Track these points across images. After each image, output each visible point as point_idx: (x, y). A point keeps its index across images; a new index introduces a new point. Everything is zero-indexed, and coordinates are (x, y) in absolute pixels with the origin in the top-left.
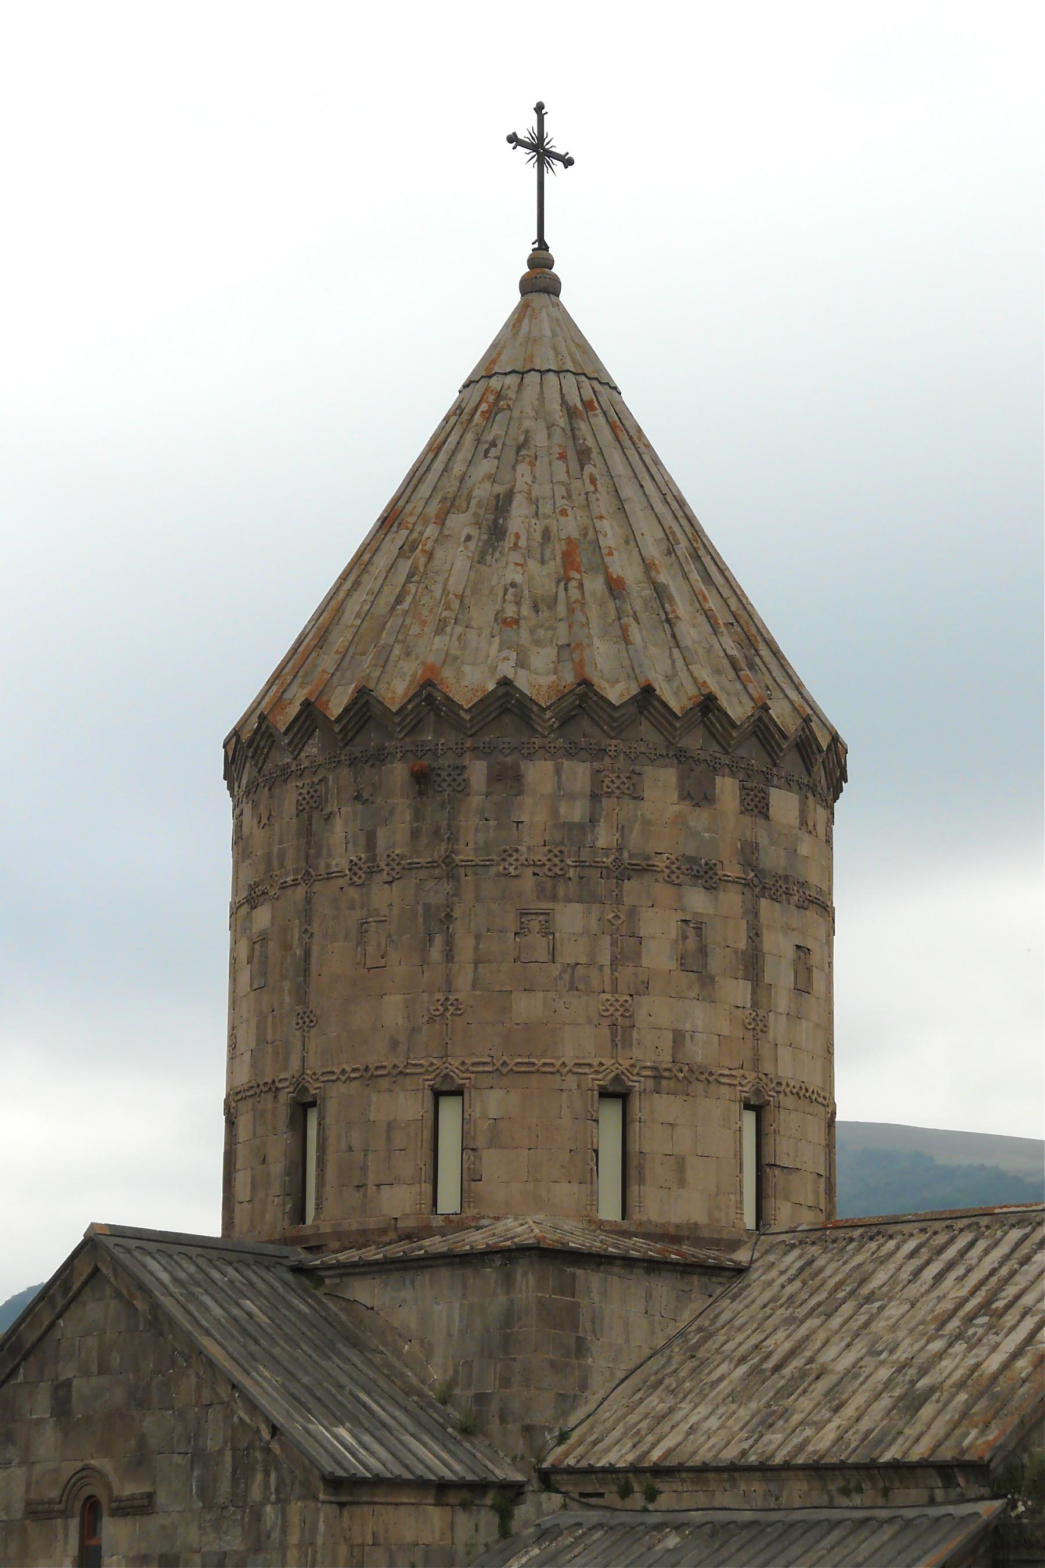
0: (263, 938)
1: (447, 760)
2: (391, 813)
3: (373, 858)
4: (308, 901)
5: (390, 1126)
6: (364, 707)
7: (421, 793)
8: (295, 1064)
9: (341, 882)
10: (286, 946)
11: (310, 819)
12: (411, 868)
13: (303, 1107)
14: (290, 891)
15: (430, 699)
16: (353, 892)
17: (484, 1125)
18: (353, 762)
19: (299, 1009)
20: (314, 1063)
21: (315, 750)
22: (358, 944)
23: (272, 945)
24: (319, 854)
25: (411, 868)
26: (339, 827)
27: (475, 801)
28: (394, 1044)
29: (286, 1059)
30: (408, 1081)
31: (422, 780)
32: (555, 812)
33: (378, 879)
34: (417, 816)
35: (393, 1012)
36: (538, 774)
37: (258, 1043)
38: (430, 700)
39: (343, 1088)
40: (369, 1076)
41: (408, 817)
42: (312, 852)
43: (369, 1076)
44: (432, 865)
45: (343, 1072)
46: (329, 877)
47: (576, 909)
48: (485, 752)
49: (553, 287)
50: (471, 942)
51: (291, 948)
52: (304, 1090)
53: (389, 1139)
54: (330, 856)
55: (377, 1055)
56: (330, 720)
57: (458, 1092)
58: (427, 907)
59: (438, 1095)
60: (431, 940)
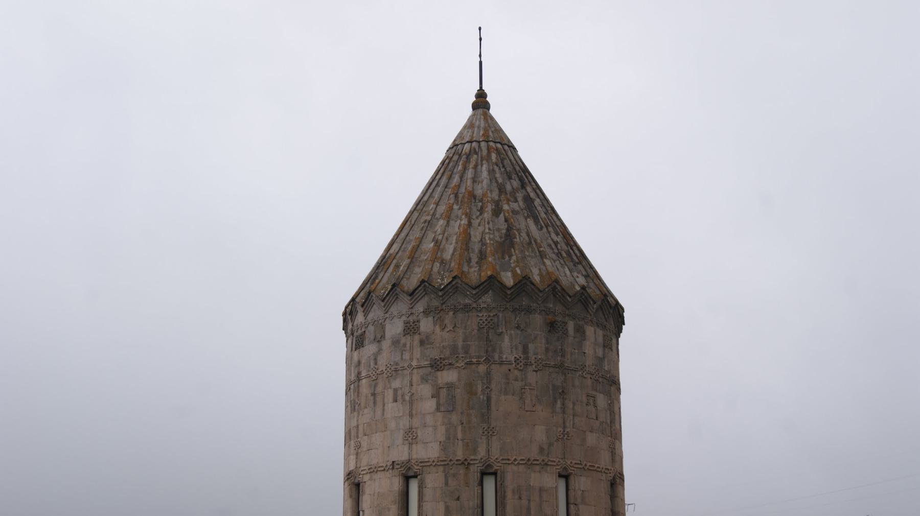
0: (450, 386)
1: (559, 319)
2: (535, 338)
3: (527, 358)
4: (488, 374)
5: (541, 490)
6: (524, 284)
7: (550, 331)
8: (482, 452)
9: (510, 367)
10: (472, 393)
11: (488, 333)
12: (546, 366)
13: (483, 474)
14: (474, 366)
15: (555, 289)
16: (516, 372)
17: (580, 493)
18: (514, 310)
19: (485, 425)
20: (495, 453)
21: (489, 300)
22: (521, 398)
23: (459, 392)
24: (494, 350)
25: (546, 366)
26: (507, 339)
27: (571, 339)
28: (541, 450)
29: (475, 451)
30: (549, 468)
31: (552, 326)
32: (595, 352)
33: (530, 368)
34: (547, 342)
35: (540, 434)
36: (590, 330)
37: (448, 438)
38: (554, 288)
39: (515, 468)
40: (529, 464)
41: (544, 341)
42: (490, 349)
43: (529, 464)
44: (555, 366)
45: (515, 460)
46: (501, 363)
47: (602, 395)
48: (574, 318)
49: (487, 106)
50: (571, 406)
51: (476, 394)
52: (489, 466)
53: (540, 496)
54: (501, 352)
55: (534, 453)
56: (505, 286)
57: (565, 476)
58: (554, 386)
59: (560, 476)
60: (556, 402)
